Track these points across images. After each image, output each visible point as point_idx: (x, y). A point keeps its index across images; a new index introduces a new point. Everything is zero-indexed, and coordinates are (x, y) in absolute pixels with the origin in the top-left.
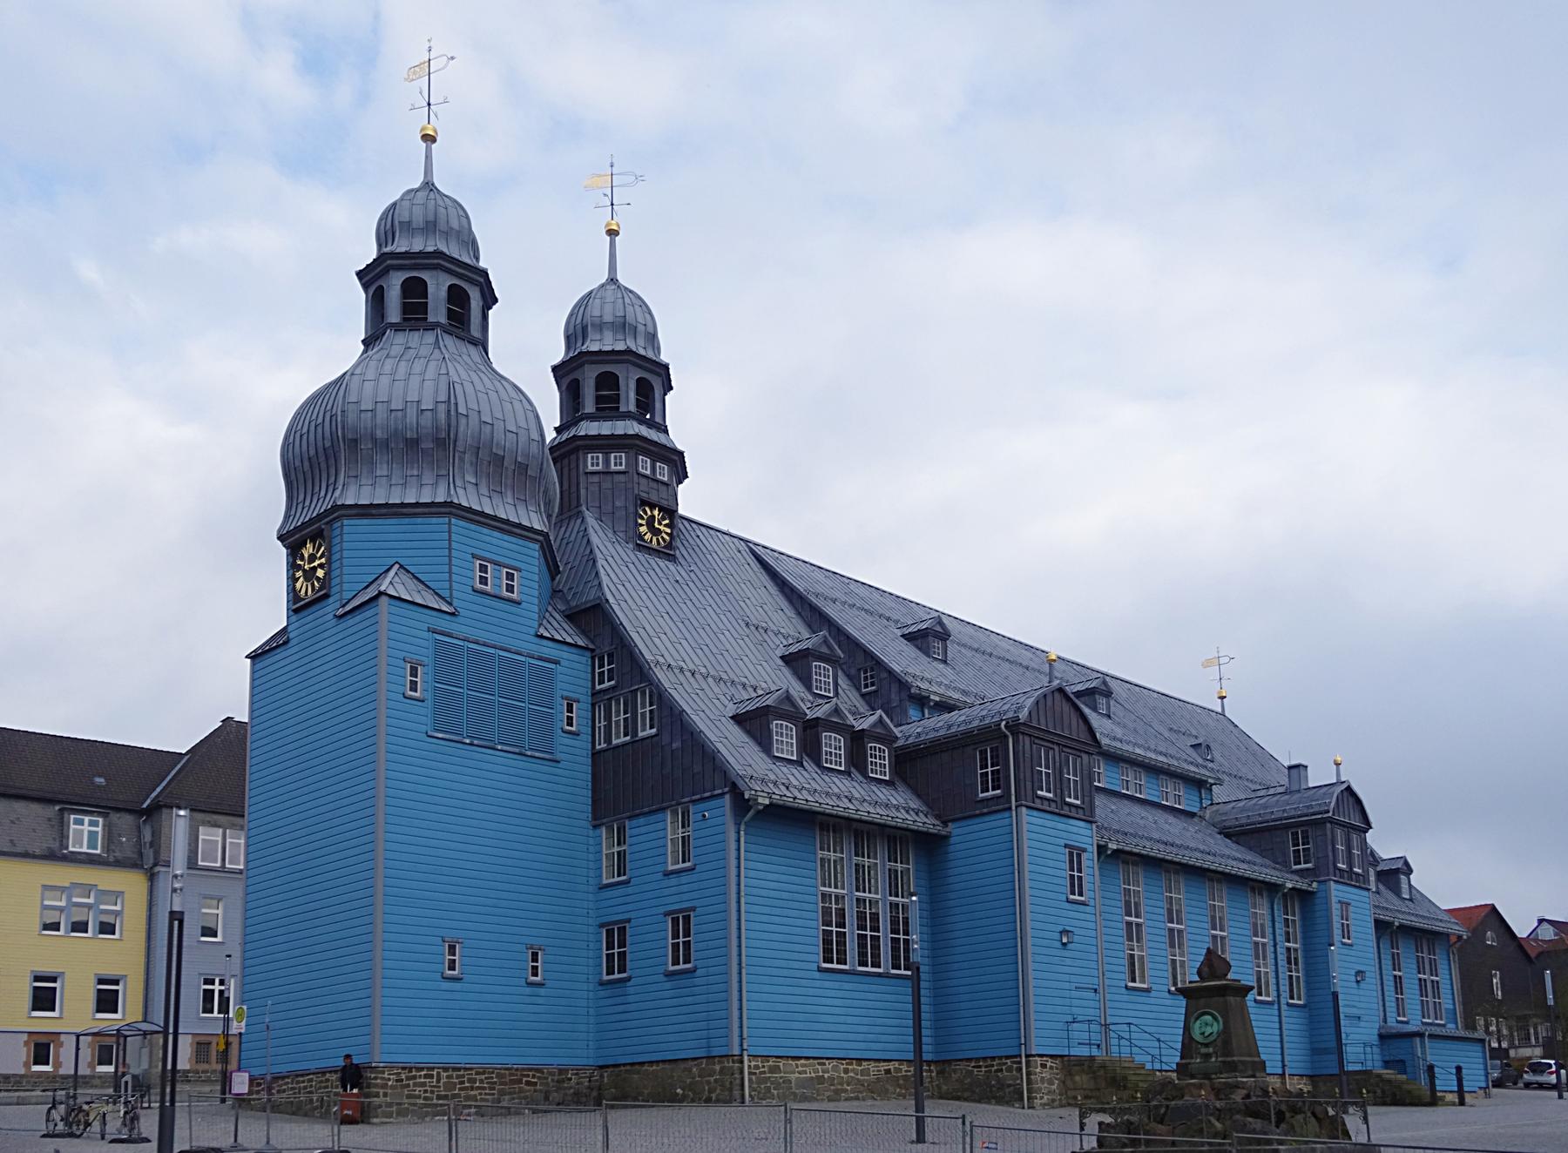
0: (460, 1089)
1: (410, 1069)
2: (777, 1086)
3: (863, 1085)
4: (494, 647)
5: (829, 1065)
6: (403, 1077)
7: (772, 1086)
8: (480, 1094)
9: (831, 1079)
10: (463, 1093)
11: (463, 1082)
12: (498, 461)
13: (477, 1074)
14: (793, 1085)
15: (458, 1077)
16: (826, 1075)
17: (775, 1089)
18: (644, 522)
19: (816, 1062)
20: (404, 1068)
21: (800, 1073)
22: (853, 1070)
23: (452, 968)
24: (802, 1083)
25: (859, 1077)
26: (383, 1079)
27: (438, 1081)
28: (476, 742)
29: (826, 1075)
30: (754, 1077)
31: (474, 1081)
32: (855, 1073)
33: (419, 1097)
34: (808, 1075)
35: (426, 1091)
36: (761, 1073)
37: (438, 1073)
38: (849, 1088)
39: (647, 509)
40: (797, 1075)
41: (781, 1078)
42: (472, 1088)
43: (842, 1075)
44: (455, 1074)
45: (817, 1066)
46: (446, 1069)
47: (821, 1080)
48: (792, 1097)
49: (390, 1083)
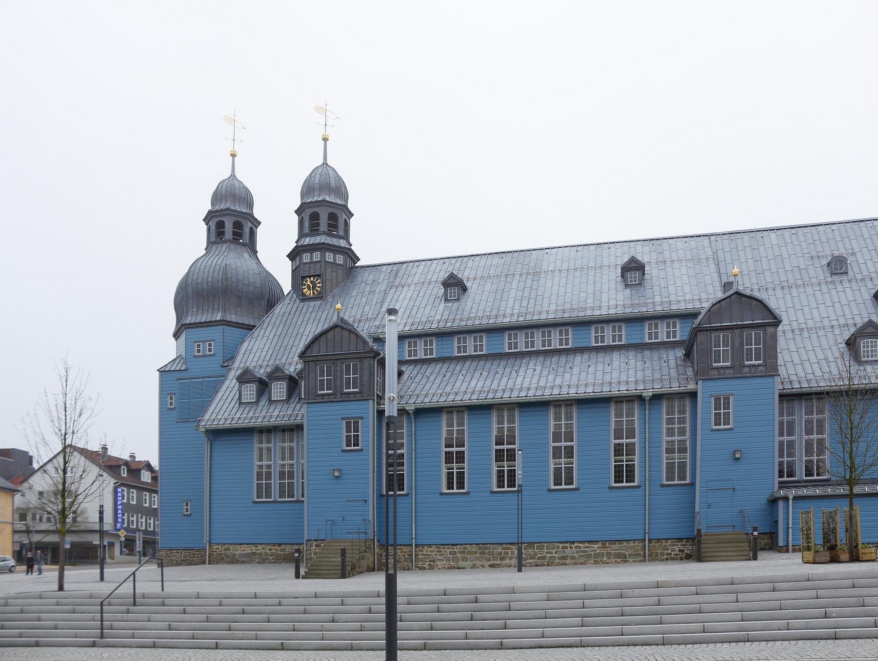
0: (190, 557)
1: (171, 550)
2: (228, 556)
3: (281, 556)
5: (260, 547)
6: (168, 553)
7: (225, 557)
8: (197, 559)
9: (261, 554)
10: (191, 559)
11: (190, 555)
13: (196, 552)
14: (237, 556)
15: (188, 553)
16: (258, 552)
17: (226, 558)
19: (252, 546)
20: (168, 550)
21: (242, 551)
22: (275, 549)
23: (187, 511)
24: (241, 555)
25: (278, 552)
26: (161, 553)
27: (181, 554)
29: (258, 552)
30: (215, 553)
31: (195, 554)
32: (276, 551)
33: (174, 560)
34: (247, 552)
35: (176, 558)
36: (219, 551)
37: (181, 552)
38: (271, 558)
40: (240, 552)
41: (230, 553)
42: (194, 557)
43: (268, 551)
44: (187, 552)
45: (253, 548)
46: (184, 550)
47: (254, 554)
48: (236, 562)
49: (164, 555)
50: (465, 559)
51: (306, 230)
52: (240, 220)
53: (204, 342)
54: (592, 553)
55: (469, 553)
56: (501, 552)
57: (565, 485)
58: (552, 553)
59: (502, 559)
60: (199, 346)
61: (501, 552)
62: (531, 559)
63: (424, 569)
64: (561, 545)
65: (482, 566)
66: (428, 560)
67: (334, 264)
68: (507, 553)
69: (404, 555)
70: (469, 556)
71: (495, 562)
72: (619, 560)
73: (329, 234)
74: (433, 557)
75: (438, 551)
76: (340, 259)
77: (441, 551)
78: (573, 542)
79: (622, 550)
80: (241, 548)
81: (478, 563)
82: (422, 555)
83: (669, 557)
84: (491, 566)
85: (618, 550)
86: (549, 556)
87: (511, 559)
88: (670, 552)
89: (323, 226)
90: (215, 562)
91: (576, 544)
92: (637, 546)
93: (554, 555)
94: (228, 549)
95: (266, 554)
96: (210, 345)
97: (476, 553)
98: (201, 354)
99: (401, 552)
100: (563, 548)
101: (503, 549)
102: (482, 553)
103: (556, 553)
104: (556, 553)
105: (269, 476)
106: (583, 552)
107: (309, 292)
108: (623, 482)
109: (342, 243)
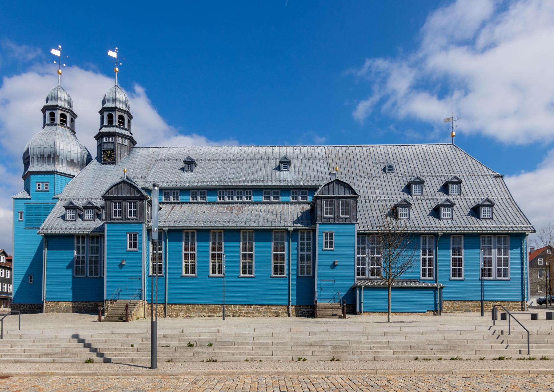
2: (57, 308)
4: (42, 204)
12: (43, 156)
16: (76, 306)
18: (105, 156)
24: (65, 308)
28: (36, 228)
29: (76, 306)
30: (49, 307)
39: (107, 152)
40: (65, 306)
50: (195, 312)
51: (106, 123)
52: (65, 113)
53: (43, 183)
54: (262, 311)
55: (197, 309)
56: (214, 309)
57: (248, 274)
58: (241, 310)
59: (215, 313)
60: (39, 185)
61: (214, 309)
62: (230, 313)
63: (173, 317)
64: (245, 306)
65: (204, 316)
66: (174, 312)
67: (122, 145)
68: (217, 309)
69: (161, 309)
70: (197, 310)
71: (211, 314)
72: (276, 315)
73: (119, 127)
74: (177, 311)
75: (180, 307)
76: (126, 142)
77: (182, 308)
78: (252, 305)
79: (277, 310)
80: (65, 303)
81: (202, 314)
82: (171, 309)
83: (302, 315)
84: (209, 316)
85: (275, 310)
86: (239, 311)
87: (219, 312)
88: (302, 312)
89: (116, 122)
90: (49, 312)
91: (254, 306)
92: (285, 308)
93: (242, 311)
94: (58, 304)
95: (81, 307)
96: (47, 185)
97: (201, 309)
98: (41, 189)
99: (160, 307)
100: (247, 307)
101: (215, 307)
102: (204, 309)
103: (243, 310)
104: (243, 310)
105: (83, 262)
106: (257, 310)
107: (107, 159)
108: (278, 274)
109: (127, 133)
